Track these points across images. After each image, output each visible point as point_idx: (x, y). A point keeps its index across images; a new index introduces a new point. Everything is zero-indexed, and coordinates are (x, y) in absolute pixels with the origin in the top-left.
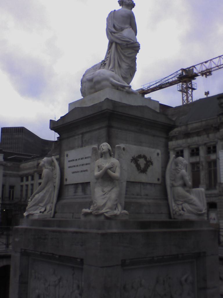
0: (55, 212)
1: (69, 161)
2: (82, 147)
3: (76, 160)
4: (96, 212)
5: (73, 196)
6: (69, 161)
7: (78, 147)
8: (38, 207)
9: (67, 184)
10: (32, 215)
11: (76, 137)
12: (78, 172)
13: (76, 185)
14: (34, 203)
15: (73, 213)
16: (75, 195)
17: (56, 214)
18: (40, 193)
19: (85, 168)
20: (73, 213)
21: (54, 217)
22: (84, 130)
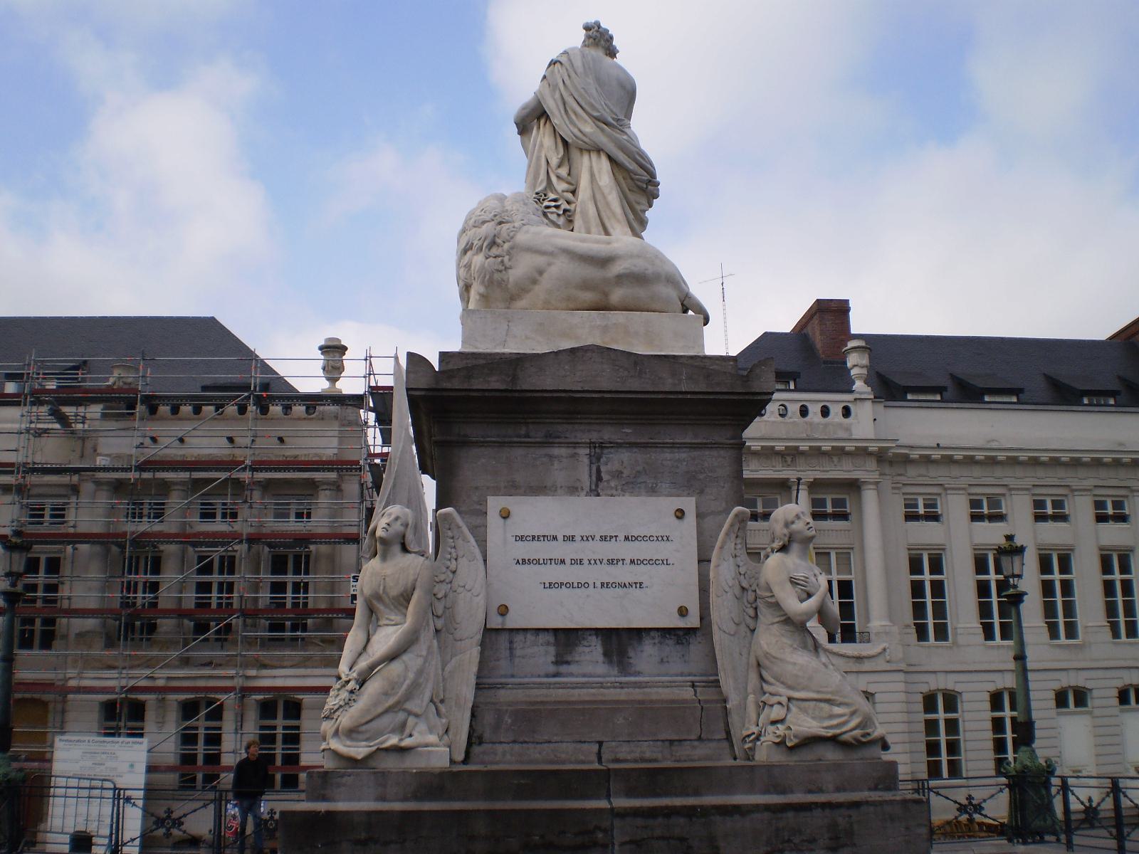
0: (474, 738)
1: (522, 538)
2: (598, 495)
3: (571, 538)
4: (863, 736)
5: (547, 676)
6: (522, 538)
7: (573, 490)
8: (401, 716)
9: (509, 625)
10: (400, 750)
11: (556, 451)
12: (585, 585)
13: (567, 639)
14: (391, 701)
15: (600, 743)
16: (556, 675)
17: (476, 749)
18: (405, 657)
19: (624, 573)
20: (600, 743)
21: (465, 761)
22: (608, 434)
